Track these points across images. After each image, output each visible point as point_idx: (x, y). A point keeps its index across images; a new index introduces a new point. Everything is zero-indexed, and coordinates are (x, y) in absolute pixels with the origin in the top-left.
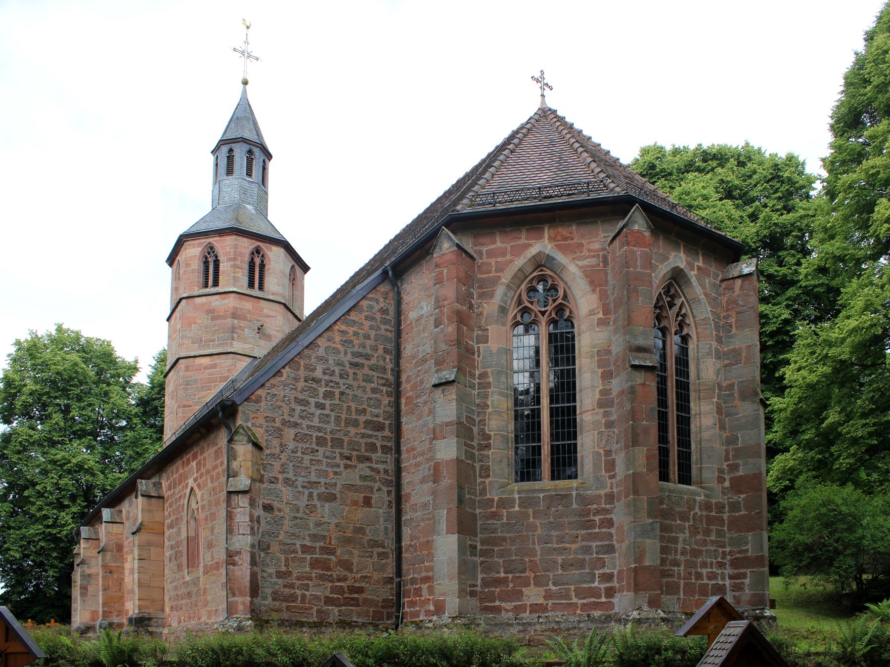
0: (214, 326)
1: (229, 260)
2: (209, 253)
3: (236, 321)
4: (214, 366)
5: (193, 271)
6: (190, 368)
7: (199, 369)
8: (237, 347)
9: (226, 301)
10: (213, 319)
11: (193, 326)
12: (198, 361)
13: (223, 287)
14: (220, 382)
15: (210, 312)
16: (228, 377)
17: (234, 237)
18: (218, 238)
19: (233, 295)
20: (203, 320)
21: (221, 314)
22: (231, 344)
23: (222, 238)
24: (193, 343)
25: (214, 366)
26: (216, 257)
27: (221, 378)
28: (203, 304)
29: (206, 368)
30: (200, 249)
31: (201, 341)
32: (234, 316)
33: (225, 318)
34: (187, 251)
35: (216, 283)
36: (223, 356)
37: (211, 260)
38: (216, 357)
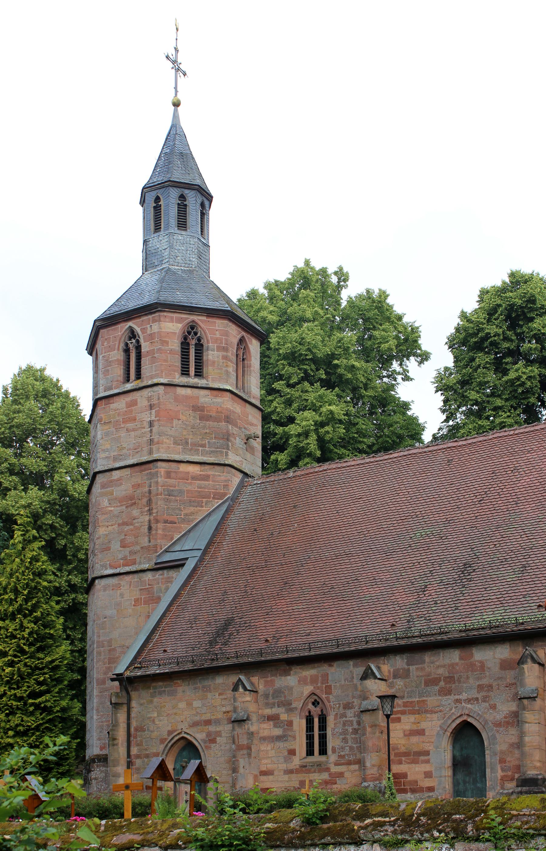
0: (204, 427)
1: (219, 349)
2: (189, 333)
3: (230, 427)
4: (206, 478)
5: (172, 352)
6: (173, 475)
7: (186, 477)
8: (232, 459)
9: (219, 400)
10: (202, 418)
11: (175, 422)
12: (183, 468)
13: (213, 380)
14: (214, 498)
15: (197, 408)
16: (225, 494)
17: (226, 322)
18: (204, 318)
19: (228, 394)
20: (188, 417)
21: (214, 414)
22: (227, 454)
23: (210, 320)
24: (175, 443)
25: (206, 478)
26: (199, 340)
27: (215, 494)
28: (187, 397)
29: (194, 478)
30: (180, 326)
31: (187, 443)
32: (228, 419)
33: (217, 420)
34: (163, 324)
35: (199, 374)
36: (217, 467)
37: (193, 342)
38: (207, 467)
